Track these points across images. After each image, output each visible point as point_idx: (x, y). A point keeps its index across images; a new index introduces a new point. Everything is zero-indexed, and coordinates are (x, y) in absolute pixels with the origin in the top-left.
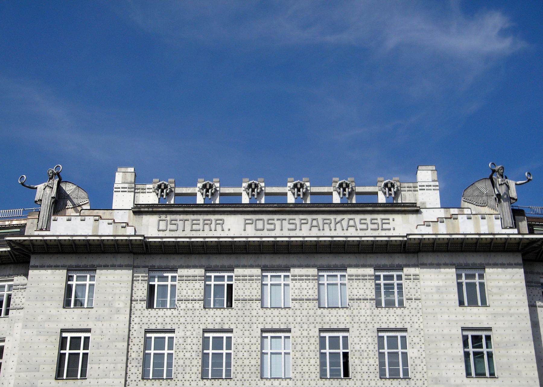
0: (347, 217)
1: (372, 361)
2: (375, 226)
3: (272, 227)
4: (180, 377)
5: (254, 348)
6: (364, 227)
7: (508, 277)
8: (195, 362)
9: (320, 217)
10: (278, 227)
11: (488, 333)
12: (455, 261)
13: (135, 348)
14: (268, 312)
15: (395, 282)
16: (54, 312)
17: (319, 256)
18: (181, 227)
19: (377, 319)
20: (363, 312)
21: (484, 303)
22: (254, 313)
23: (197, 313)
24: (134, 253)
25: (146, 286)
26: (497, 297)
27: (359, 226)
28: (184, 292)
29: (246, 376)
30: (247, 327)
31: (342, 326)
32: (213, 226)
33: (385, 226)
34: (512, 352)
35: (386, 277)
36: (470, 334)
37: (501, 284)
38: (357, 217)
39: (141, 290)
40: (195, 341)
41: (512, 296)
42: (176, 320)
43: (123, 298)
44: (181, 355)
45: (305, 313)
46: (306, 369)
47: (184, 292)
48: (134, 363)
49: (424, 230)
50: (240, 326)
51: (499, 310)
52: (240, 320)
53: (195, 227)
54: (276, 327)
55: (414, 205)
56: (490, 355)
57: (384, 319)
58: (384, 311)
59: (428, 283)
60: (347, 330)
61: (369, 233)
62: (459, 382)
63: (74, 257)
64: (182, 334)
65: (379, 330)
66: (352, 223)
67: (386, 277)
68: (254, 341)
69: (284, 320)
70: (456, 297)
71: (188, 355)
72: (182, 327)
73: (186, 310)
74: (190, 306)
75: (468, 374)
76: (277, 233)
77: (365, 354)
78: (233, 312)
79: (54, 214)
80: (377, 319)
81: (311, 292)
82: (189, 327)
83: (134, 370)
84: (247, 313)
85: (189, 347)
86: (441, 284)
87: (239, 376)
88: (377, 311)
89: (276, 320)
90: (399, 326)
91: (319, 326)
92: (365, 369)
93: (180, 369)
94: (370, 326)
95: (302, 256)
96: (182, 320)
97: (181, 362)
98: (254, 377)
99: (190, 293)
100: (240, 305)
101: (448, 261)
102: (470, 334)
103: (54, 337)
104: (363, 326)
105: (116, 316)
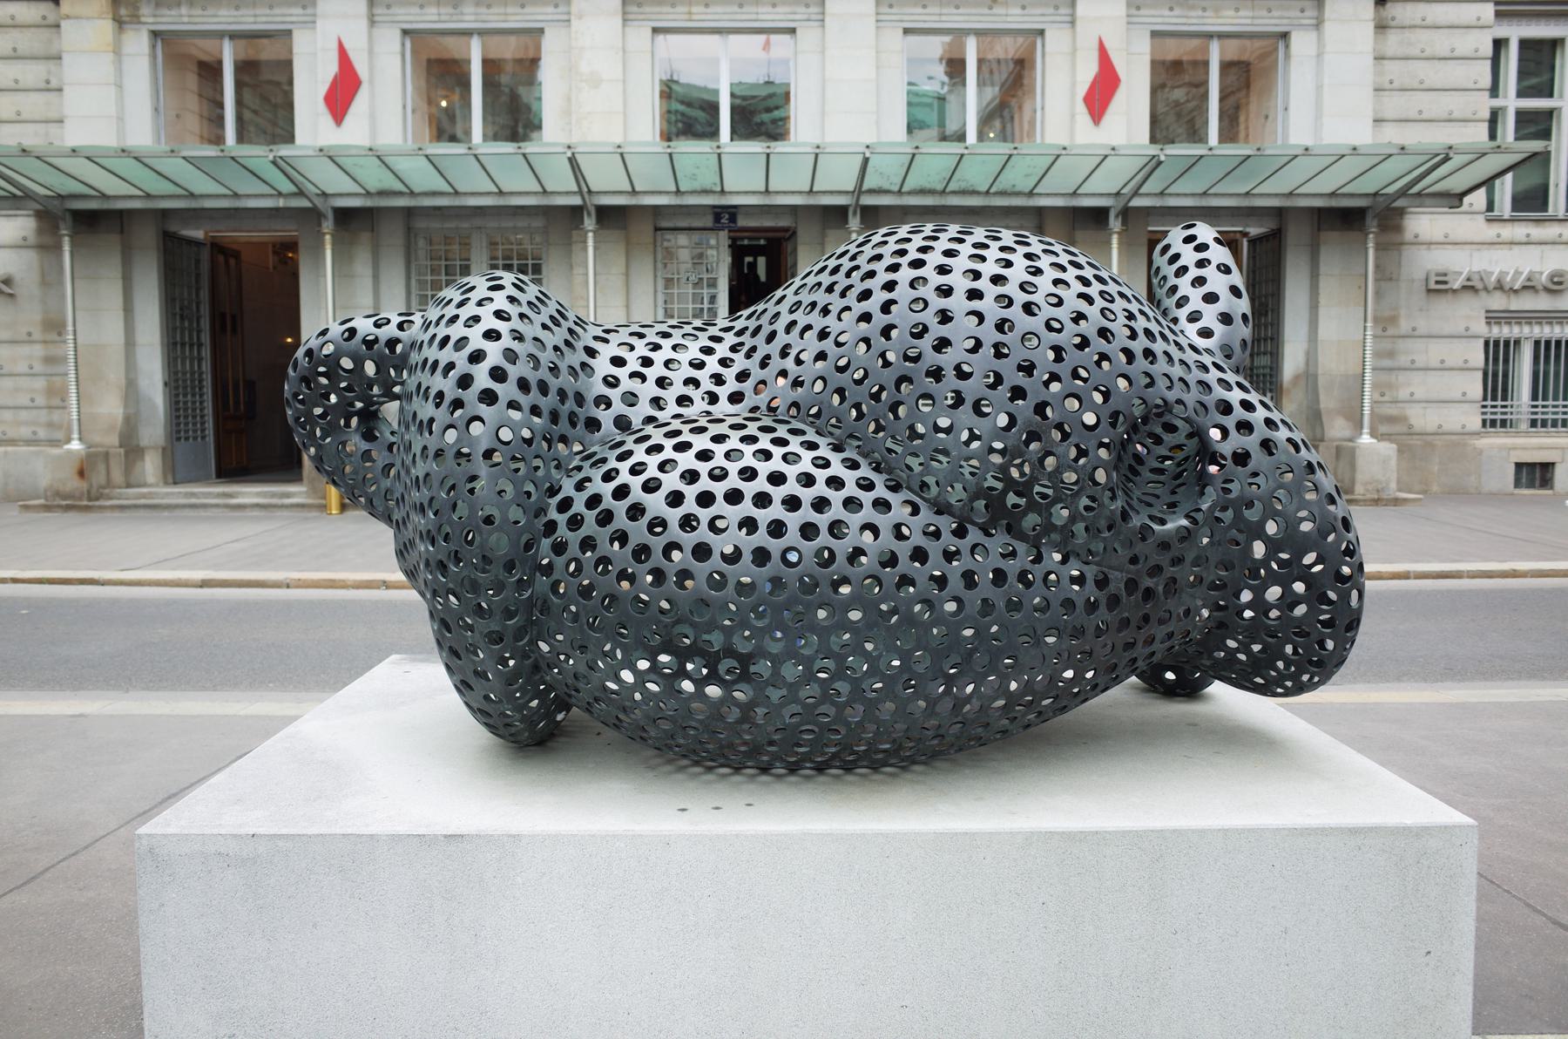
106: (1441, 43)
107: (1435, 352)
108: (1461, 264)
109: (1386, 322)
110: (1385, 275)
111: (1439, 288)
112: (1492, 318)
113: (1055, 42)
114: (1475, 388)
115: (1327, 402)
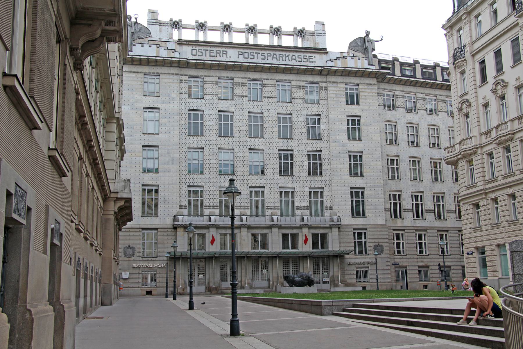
0: (291, 54)
2: (305, 60)
3: (252, 57)
4: (207, 135)
5: (245, 121)
6: (300, 60)
7: (370, 91)
8: (215, 128)
9: (278, 53)
10: (256, 57)
11: (359, 118)
13: (183, 119)
14: (252, 103)
16: (139, 97)
17: (277, 74)
18: (204, 54)
19: (306, 109)
20: (299, 105)
21: (358, 104)
22: (244, 103)
23: (215, 102)
24: (180, 67)
25: (187, 86)
26: (364, 101)
27: (298, 59)
28: (208, 90)
29: (241, 136)
30: (241, 110)
31: (289, 112)
32: (221, 54)
33: (311, 60)
34: (369, 128)
36: (350, 118)
37: (366, 94)
38: (297, 54)
39: (185, 88)
40: (214, 116)
41: (371, 101)
42: (204, 105)
43: (176, 92)
45: (270, 104)
46: (271, 133)
47: (208, 90)
48: (183, 127)
49: (330, 64)
50: (237, 110)
51: (364, 107)
52: (238, 106)
53: (212, 54)
54: (256, 111)
56: (359, 129)
57: (310, 109)
58: (309, 105)
59: (331, 92)
60: (291, 114)
61: (302, 63)
63: (147, 67)
64: (208, 113)
65: (307, 115)
66: (294, 57)
68: (245, 118)
69: (260, 107)
71: (211, 124)
74: (211, 98)
75: (349, 139)
76: (255, 61)
78: (234, 102)
80: (306, 109)
81: (273, 93)
82: (211, 109)
83: (183, 130)
84: (241, 103)
85: (211, 120)
86: (338, 92)
87: (238, 136)
88: (306, 105)
89: (256, 107)
90: (317, 113)
92: (300, 134)
93: (207, 131)
94: (303, 113)
95: (268, 73)
96: (207, 105)
97: (207, 127)
98: (245, 136)
102: (350, 118)
103: (140, 111)
104: (299, 112)
105: (173, 101)
106: (347, 233)
107: (350, 272)
108: (352, 261)
109: (342, 269)
110: (342, 263)
111: (349, 264)
112: (357, 268)
113: (300, 234)
114: (355, 277)
115: (336, 279)
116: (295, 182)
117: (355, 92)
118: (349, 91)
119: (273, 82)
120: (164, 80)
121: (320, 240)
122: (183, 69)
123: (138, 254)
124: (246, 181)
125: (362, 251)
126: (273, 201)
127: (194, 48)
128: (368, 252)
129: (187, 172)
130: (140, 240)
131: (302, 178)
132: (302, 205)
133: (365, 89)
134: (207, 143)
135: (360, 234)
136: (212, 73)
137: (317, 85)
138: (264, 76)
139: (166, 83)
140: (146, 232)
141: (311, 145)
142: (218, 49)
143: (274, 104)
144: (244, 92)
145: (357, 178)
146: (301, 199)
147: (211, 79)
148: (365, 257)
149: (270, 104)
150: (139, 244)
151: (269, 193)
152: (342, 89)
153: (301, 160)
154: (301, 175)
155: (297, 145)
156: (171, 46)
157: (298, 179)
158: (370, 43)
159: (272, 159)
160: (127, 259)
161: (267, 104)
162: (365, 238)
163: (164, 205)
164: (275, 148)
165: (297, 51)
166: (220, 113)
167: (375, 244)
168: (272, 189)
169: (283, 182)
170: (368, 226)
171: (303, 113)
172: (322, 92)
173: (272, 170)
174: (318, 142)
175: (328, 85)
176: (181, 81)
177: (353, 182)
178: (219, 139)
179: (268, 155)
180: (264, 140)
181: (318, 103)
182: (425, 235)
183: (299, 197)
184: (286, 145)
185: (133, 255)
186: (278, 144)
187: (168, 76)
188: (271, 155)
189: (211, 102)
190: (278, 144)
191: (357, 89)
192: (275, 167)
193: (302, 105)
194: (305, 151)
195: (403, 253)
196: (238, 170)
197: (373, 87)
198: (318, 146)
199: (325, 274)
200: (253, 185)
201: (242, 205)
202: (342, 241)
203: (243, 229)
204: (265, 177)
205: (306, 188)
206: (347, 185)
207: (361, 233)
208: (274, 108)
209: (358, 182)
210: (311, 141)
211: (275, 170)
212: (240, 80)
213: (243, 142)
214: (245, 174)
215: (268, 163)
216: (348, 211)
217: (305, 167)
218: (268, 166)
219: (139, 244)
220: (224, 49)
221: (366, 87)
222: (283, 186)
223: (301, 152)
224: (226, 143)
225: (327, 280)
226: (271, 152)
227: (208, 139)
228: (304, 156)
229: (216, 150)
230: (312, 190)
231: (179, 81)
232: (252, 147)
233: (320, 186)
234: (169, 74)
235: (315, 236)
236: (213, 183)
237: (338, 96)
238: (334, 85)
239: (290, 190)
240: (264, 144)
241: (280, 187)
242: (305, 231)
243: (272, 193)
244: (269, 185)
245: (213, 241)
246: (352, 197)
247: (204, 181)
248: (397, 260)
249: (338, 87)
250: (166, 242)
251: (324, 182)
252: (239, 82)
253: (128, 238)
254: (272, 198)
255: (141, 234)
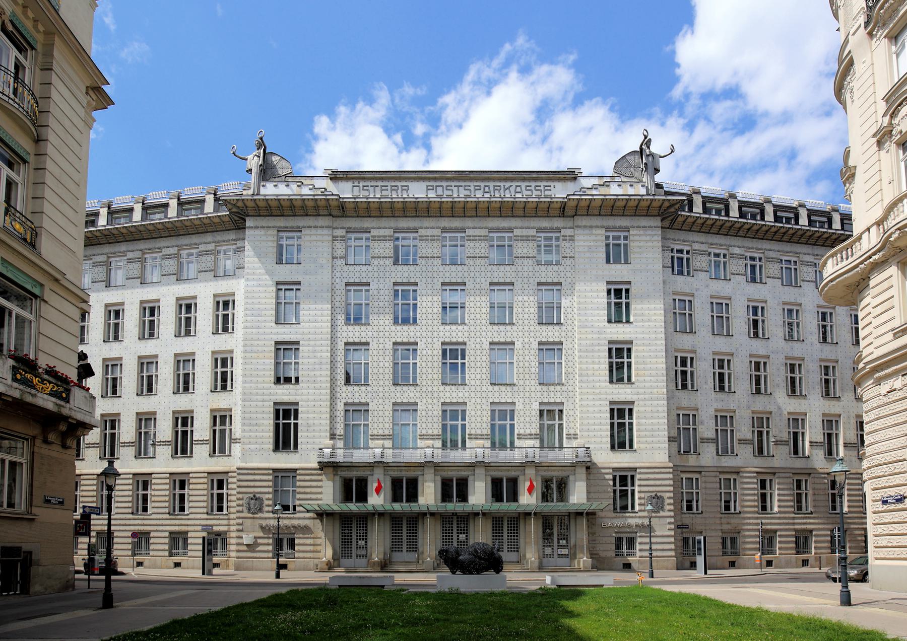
0: (514, 184)
1: (532, 310)
7: (648, 238)
9: (491, 184)
12: (605, 224)
13: (338, 299)
14: (447, 268)
15: (554, 243)
20: (526, 268)
22: (435, 269)
28: (376, 251)
29: (430, 322)
30: (429, 280)
31: (508, 280)
33: (548, 193)
35: (546, 239)
37: (642, 244)
40: (387, 292)
42: (370, 275)
43: (325, 255)
44: (376, 304)
46: (478, 316)
47: (376, 251)
48: (338, 310)
50: (424, 280)
52: (424, 274)
54: (454, 280)
55: (571, 172)
57: (543, 274)
58: (543, 268)
59: (581, 243)
62: (602, 324)
65: (539, 284)
66: (518, 189)
67: (546, 239)
69: (460, 275)
70: (604, 255)
71: (381, 304)
72: (376, 280)
73: (379, 266)
74: (382, 263)
75: (609, 321)
77: (527, 304)
78: (418, 268)
79: (263, 181)
80: (537, 274)
81: (483, 251)
82: (382, 280)
84: (430, 269)
85: (382, 298)
86: (592, 244)
87: (424, 322)
88: (537, 268)
89: (454, 274)
90: (556, 280)
91: (489, 280)
92: (526, 316)
94: (531, 280)
96: (376, 275)
98: (436, 322)
99: (381, 251)
100: (424, 262)
101: (599, 224)
104: (526, 280)
116: (516, 395)
117: (622, 242)
118: (611, 242)
119: (484, 232)
120: (308, 238)
121: (555, 486)
122: (338, 219)
123: (266, 509)
124: (436, 395)
125: (627, 505)
126: (479, 425)
127: (356, 184)
128: (637, 508)
129: (343, 382)
130: (269, 487)
131: (527, 389)
132: (528, 432)
133: (640, 235)
134: (375, 334)
135: (624, 479)
136: (384, 222)
137: (558, 235)
138: (468, 222)
139: (310, 241)
140: (280, 475)
141: (544, 334)
142: (393, 184)
143: (483, 268)
144: (435, 251)
145: (622, 386)
146: (526, 422)
147: (382, 232)
148: (631, 515)
149: (477, 269)
150: (269, 493)
151: (473, 413)
152: (599, 238)
153: (527, 358)
154: (527, 383)
155: (521, 334)
156: (319, 183)
157: (521, 389)
158: (650, 158)
159: (478, 358)
160: (251, 515)
161: (472, 268)
162: (633, 485)
163: (306, 434)
164: (484, 340)
165: (524, 179)
166: (396, 288)
167: (649, 494)
168: (479, 407)
169: (497, 394)
170: (638, 465)
171: (531, 280)
172: (564, 244)
173: (478, 376)
174: (557, 328)
175: (576, 232)
176: (334, 239)
177: (615, 391)
178: (393, 328)
179: (472, 352)
180: (465, 327)
181: (558, 263)
182: (735, 480)
183: (522, 419)
184: (503, 334)
185: (260, 510)
186: (490, 334)
187: (313, 231)
188: (478, 352)
189: (382, 269)
190: (490, 334)
191: (626, 238)
192: (484, 370)
193: (531, 268)
194: (534, 343)
195: (697, 509)
196: (424, 377)
197: (654, 233)
198: (557, 334)
199: (563, 542)
200: (448, 401)
201: (430, 432)
202: (592, 489)
203: (427, 470)
204: (466, 387)
205: (535, 404)
206: (603, 397)
207: (626, 476)
208: (483, 274)
209: (622, 393)
210: (544, 327)
211: (484, 376)
212: (429, 232)
213: (433, 331)
214: (436, 383)
215: (473, 364)
216: (604, 440)
217: (533, 370)
218: (473, 370)
219: (269, 493)
220: (404, 183)
221: (642, 232)
222: (496, 400)
223: (527, 346)
224: (405, 334)
225: (565, 551)
226: (478, 346)
227: (376, 328)
228: (532, 352)
229: (389, 346)
230: (546, 408)
231: (330, 238)
232: (447, 340)
233: (558, 400)
234: (316, 227)
235: (547, 483)
236: (384, 398)
237: (594, 249)
238: (587, 231)
239: (508, 408)
240: (466, 334)
241: (491, 403)
242: (530, 472)
243: (479, 413)
244: (473, 400)
245: (378, 490)
246: (612, 417)
247: (370, 395)
248: (686, 521)
249: (592, 234)
250: (308, 490)
251: (565, 394)
252: (428, 234)
253: (252, 484)
254: (478, 421)
255: (270, 477)
